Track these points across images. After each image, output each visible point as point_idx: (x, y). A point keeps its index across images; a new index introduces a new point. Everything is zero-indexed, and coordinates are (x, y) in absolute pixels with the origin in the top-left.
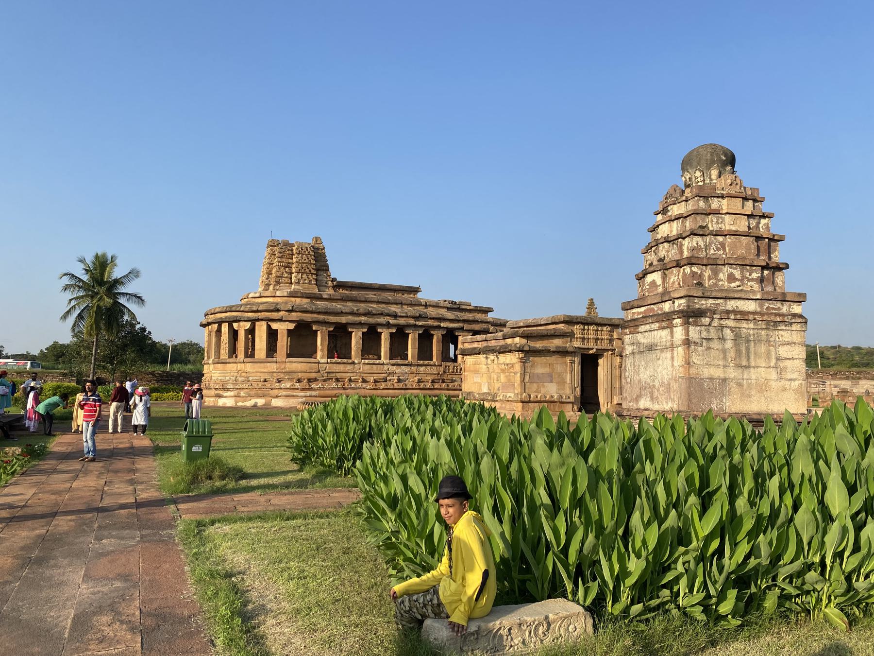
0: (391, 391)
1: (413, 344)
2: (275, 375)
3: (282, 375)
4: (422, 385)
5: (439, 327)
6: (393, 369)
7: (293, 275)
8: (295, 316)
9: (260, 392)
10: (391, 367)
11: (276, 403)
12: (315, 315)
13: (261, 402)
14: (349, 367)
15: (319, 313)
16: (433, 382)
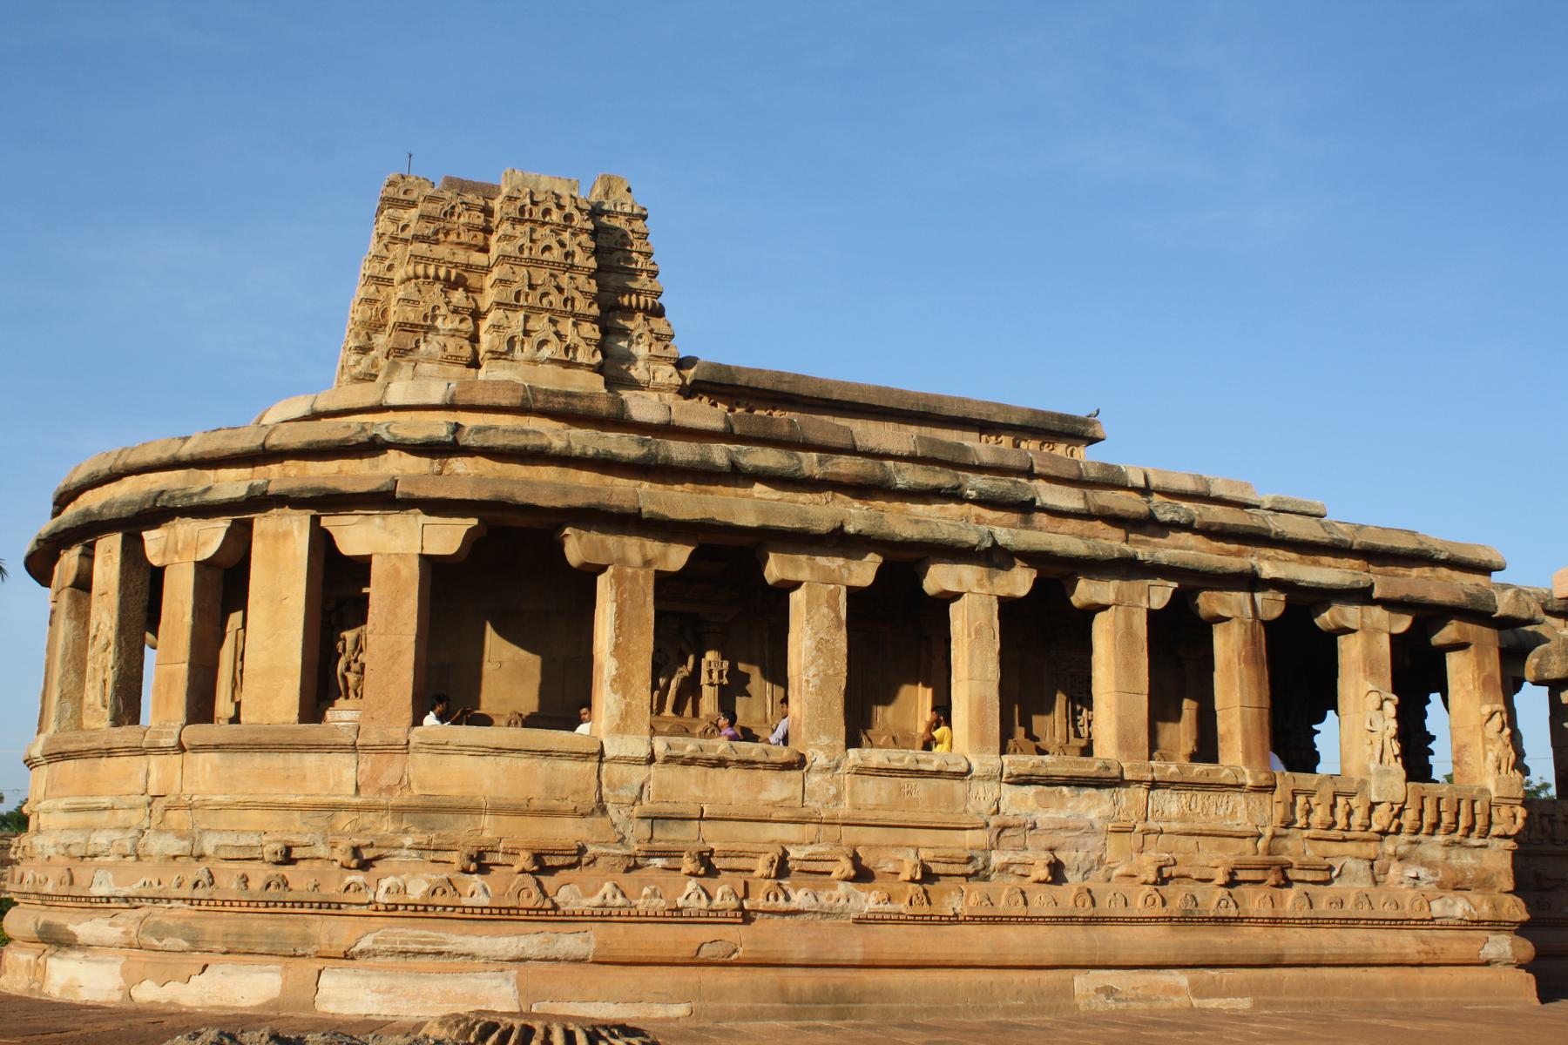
0: (1011, 933)
1: (1127, 665)
2: (344, 821)
3: (387, 826)
4: (1177, 897)
5: (1250, 582)
6: (1021, 802)
7: (484, 325)
8: (467, 476)
9: (259, 924)
10: (1009, 793)
11: (347, 995)
12: (585, 478)
13: (246, 987)
14: (778, 788)
15: (606, 464)
16: (1232, 883)
